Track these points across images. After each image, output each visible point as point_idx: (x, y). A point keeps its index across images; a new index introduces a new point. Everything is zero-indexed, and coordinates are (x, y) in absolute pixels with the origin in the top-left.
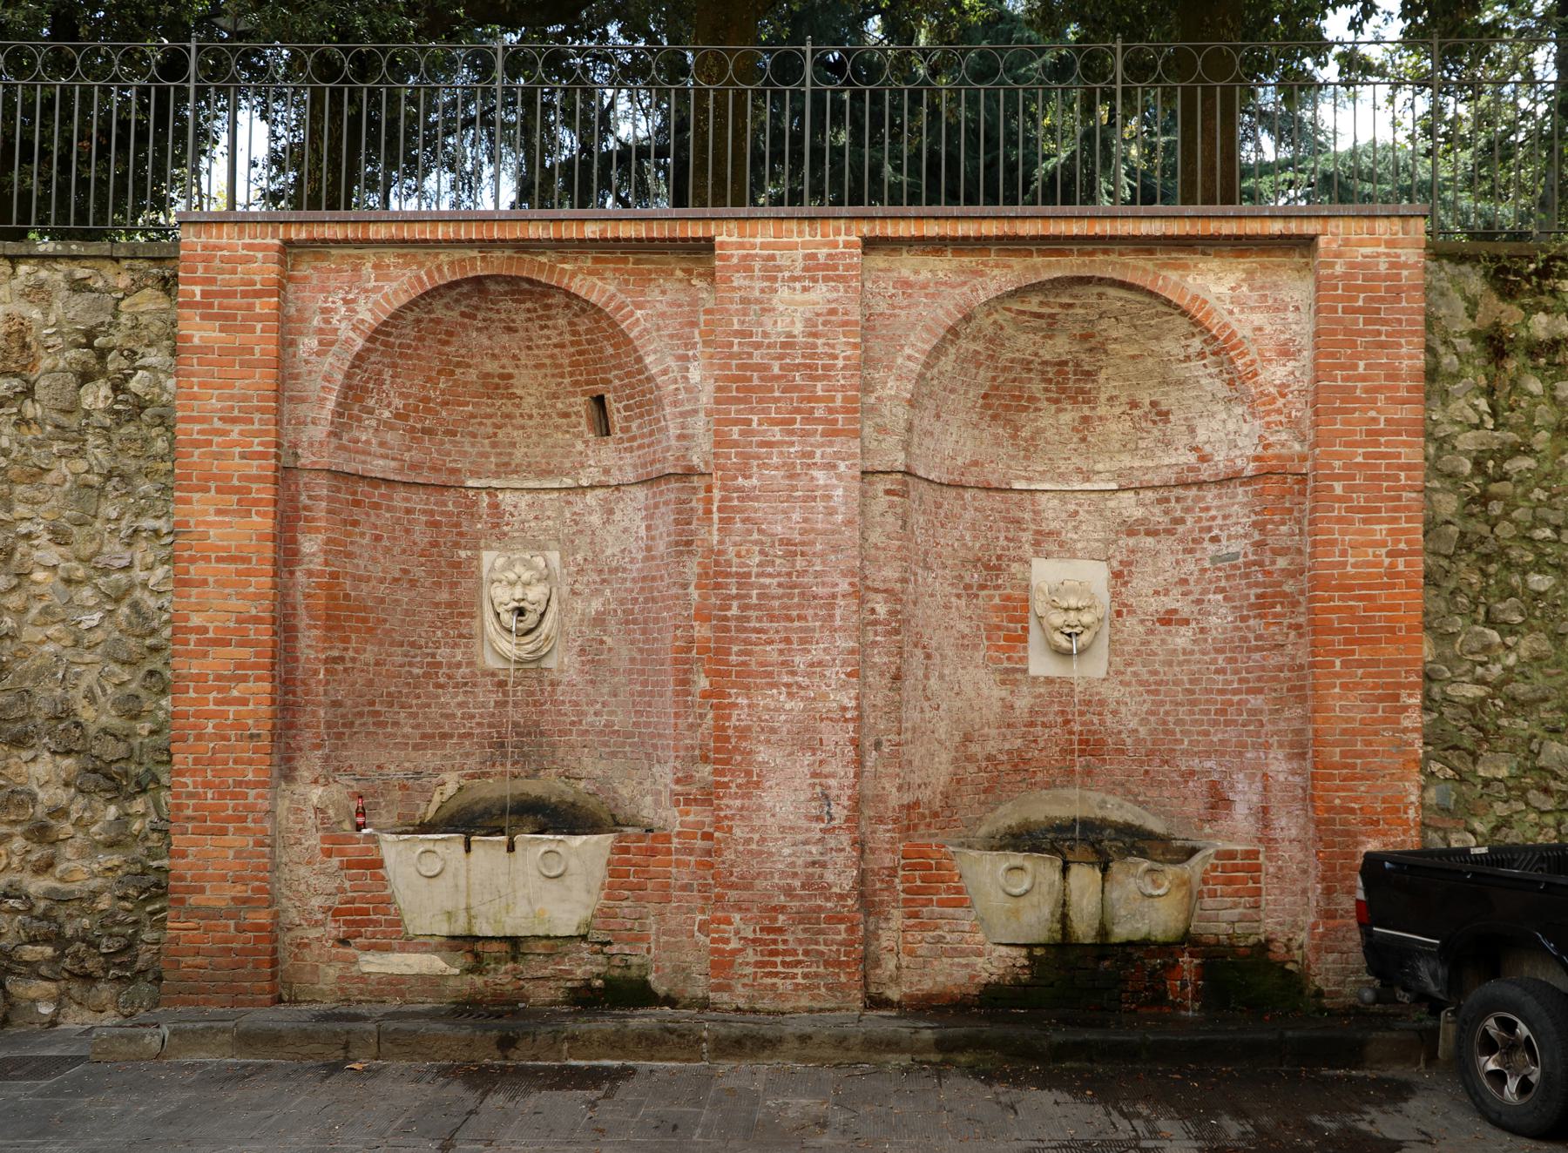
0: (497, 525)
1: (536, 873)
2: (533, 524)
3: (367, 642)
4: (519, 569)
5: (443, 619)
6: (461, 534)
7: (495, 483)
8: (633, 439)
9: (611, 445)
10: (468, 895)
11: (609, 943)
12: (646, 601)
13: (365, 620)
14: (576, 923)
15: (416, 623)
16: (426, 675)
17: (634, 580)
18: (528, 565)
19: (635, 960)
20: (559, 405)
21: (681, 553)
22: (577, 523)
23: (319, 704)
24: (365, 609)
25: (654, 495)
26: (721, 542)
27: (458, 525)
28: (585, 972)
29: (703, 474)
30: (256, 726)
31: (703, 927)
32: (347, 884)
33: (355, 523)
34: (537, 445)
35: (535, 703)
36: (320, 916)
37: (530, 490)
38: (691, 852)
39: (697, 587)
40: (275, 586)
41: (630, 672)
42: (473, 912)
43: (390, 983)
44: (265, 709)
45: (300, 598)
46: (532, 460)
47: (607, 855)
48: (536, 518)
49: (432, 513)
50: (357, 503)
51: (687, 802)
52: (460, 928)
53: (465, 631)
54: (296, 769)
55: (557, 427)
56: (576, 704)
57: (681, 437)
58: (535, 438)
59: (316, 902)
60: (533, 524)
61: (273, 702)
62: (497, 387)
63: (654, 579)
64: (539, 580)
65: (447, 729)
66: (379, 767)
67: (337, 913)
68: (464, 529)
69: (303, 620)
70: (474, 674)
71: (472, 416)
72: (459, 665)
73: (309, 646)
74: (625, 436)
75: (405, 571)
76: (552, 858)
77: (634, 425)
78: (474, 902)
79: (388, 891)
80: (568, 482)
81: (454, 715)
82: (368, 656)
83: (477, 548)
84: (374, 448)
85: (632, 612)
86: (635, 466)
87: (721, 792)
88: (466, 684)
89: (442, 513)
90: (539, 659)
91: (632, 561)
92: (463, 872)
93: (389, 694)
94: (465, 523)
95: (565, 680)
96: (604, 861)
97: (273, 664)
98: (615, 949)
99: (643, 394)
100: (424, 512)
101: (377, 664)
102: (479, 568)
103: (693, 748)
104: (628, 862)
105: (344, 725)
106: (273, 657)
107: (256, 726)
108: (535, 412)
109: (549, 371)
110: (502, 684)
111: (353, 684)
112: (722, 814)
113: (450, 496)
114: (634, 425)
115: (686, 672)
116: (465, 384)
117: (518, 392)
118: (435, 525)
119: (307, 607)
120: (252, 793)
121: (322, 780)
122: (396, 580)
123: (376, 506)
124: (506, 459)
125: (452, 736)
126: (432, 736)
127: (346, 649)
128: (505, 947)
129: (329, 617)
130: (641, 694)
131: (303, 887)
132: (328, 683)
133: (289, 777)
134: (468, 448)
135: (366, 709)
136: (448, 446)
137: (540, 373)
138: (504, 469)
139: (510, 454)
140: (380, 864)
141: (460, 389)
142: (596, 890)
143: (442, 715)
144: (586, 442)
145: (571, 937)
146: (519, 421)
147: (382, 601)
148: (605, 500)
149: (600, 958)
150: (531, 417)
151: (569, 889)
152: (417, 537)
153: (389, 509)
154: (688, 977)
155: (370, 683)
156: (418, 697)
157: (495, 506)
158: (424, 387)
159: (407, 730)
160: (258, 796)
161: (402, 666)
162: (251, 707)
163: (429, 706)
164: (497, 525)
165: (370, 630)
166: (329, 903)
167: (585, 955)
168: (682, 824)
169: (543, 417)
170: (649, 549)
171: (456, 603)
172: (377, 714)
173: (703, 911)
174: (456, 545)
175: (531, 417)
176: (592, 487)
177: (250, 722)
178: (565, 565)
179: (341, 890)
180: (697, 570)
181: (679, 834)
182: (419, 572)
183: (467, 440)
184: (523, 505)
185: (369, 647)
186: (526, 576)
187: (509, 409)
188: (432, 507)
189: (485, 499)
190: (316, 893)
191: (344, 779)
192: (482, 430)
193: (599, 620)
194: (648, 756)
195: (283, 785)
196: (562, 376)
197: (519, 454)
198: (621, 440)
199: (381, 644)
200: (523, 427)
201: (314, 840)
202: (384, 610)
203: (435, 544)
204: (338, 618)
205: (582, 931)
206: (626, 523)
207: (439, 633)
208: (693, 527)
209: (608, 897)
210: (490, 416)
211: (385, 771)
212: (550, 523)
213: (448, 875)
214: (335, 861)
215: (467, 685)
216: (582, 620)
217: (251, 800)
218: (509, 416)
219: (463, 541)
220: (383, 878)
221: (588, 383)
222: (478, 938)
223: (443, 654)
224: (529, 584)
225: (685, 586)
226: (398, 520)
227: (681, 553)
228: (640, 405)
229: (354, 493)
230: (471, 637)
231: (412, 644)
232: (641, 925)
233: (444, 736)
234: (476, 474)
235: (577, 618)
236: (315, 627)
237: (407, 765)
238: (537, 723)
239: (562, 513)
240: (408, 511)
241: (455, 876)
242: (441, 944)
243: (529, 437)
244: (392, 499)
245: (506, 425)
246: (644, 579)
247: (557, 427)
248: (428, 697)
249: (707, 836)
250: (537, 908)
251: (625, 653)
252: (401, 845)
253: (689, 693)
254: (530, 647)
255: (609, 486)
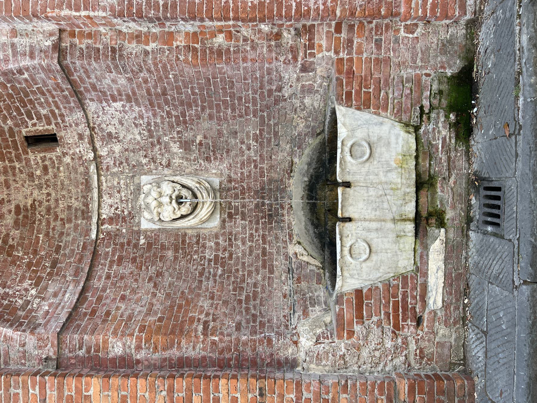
0: (124, 218)
1: (367, 165)
2: (123, 194)
3: (196, 305)
4: (150, 200)
5: (185, 254)
6: (129, 243)
7: (95, 220)
8: (52, 112)
9: (63, 133)
10: (384, 221)
11: (422, 108)
12: (167, 102)
13: (180, 307)
14: (406, 135)
15: (187, 272)
16: (223, 266)
17: (155, 115)
18: (147, 195)
19: (435, 87)
20: (38, 173)
21: (121, 56)
22: (121, 163)
23: (238, 340)
24: (172, 307)
25: (87, 91)
26: (104, 9)
27: (122, 245)
28: (444, 127)
29: (60, 39)
30: (254, 391)
31: (410, 29)
32: (375, 319)
33: (108, 313)
34: (69, 191)
35: (243, 193)
36: (400, 340)
37: (100, 196)
38: (350, 41)
39: (147, 44)
40: (145, 376)
41: (219, 119)
42: (397, 218)
43: (451, 285)
44: (241, 384)
45: (157, 356)
46: (80, 195)
47: (352, 110)
48: (119, 192)
49: (112, 262)
50: (94, 312)
51: (312, 46)
52: (410, 227)
53: (195, 240)
54: (286, 359)
55: (55, 176)
56: (243, 164)
57: (32, 56)
58: (64, 193)
59: (389, 344)
60: (123, 194)
61: (235, 377)
62: (26, 217)
63: (148, 91)
64: (159, 187)
65: (260, 252)
66: (285, 296)
67: (397, 326)
68: (125, 241)
69: (174, 353)
70: (224, 234)
71: (47, 234)
72: (217, 244)
73: (194, 348)
74: (53, 122)
75: (150, 279)
76: (357, 151)
77: (43, 112)
78: (390, 216)
79: (380, 285)
80: (93, 168)
81: (251, 247)
82: (206, 304)
83: (139, 232)
84: (56, 301)
85: (177, 117)
86: (71, 110)
87: (304, 8)
88: (230, 240)
89: (113, 255)
90: (214, 190)
91: (141, 117)
92: (366, 224)
93: (234, 290)
94: (122, 241)
95: (227, 172)
96: (358, 112)
97: (206, 377)
98: (426, 103)
99: (10, 96)
100: (110, 267)
101: (212, 298)
102: (152, 231)
103: (269, 46)
104: (358, 93)
105: (254, 321)
106: (199, 377)
107: (254, 391)
108: (44, 191)
109: (11, 178)
110: (230, 216)
111: (225, 315)
112: (322, 7)
113: (102, 250)
114: (43, 112)
115: (212, 52)
116: (23, 239)
117: (30, 202)
118: (120, 259)
119: (164, 350)
120: (306, 395)
121: (295, 338)
122: (155, 286)
123: (100, 299)
124: (79, 213)
125: (264, 249)
126: (264, 261)
127: (199, 320)
128: (423, 193)
129: (173, 332)
130: (233, 110)
131: (377, 354)
132: (222, 334)
133: (292, 364)
134: (70, 238)
135: (244, 305)
136: (67, 251)
137: (13, 185)
138: (86, 214)
139: (76, 209)
140: (359, 292)
141: (26, 242)
142: (381, 119)
143: (250, 255)
144: (65, 154)
145: (417, 139)
146: (52, 203)
147: (168, 295)
148: (102, 140)
149: (433, 115)
150: (49, 194)
151: (380, 138)
152: (127, 272)
153: (104, 290)
154: (450, 42)
155: (225, 303)
156: (237, 270)
157: (111, 220)
158: (19, 266)
159: (259, 277)
160: (308, 390)
161: (215, 282)
162: (238, 395)
163: (244, 263)
164: (124, 218)
165: (188, 303)
166: (390, 334)
167: (431, 127)
168: (328, 50)
169: (48, 186)
170: (129, 99)
171: (176, 246)
172: (247, 298)
173: (398, 31)
174: (136, 246)
175: (49, 194)
176: (95, 150)
177: (250, 396)
178: (149, 172)
179: (379, 324)
180: (134, 45)
181: (337, 52)
182: (152, 270)
183: (64, 238)
184: (110, 201)
185: (200, 304)
186: (154, 194)
187: (43, 209)
188: (108, 262)
189: (106, 227)
190: (382, 343)
191: (294, 321)
192: (58, 228)
193: (186, 146)
194: (277, 102)
195: (299, 368)
196: (14, 168)
197: (76, 204)
198: (57, 124)
199: (199, 295)
200: (57, 200)
201: (342, 346)
202: (175, 294)
203: (134, 260)
204: (174, 326)
205: (412, 130)
206: (115, 121)
207: (195, 257)
208: (101, 47)
209: (386, 109)
210: (48, 223)
211: (288, 292)
212: (122, 182)
213: (372, 235)
214: (357, 328)
215: (231, 238)
216: (187, 159)
217: (311, 396)
218: (48, 209)
219: (134, 242)
220: (370, 290)
221: (17, 149)
222: (417, 213)
223: (209, 254)
224: (160, 193)
225: (146, 53)
226: (114, 284)
227: (121, 56)
228: (21, 101)
229: (85, 314)
230: (198, 236)
231: (201, 274)
232: (408, 81)
233: (264, 253)
234: (88, 232)
235: (185, 163)
236: (179, 344)
237: (283, 278)
238: (256, 192)
239: (114, 175)
240: (108, 277)
241: (369, 230)
242: (422, 243)
243: (64, 196)
244: (97, 289)
245: (55, 213)
246: (152, 104)
247: (55, 176)
248: (238, 264)
249: (338, 29)
250: (394, 165)
251: (206, 125)
252: (346, 274)
253: (228, 50)
254: (205, 194)
255: (92, 136)
